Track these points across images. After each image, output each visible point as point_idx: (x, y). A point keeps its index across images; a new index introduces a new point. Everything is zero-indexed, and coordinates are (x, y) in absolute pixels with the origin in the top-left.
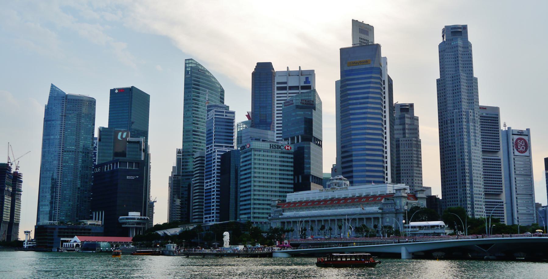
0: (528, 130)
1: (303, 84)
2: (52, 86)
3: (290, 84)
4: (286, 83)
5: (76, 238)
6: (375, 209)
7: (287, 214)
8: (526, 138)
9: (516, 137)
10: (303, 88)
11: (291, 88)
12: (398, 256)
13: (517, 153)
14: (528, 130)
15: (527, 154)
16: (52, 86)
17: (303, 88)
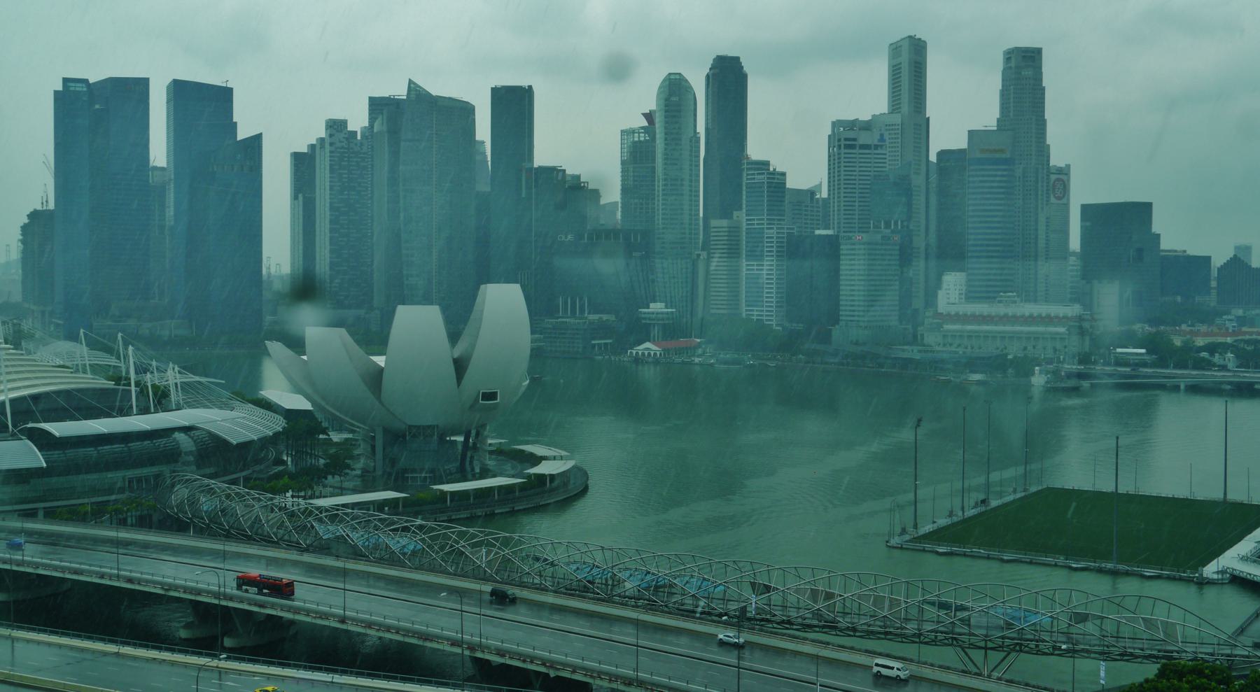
0: (1068, 166)
1: (876, 142)
2: (410, 82)
3: (861, 142)
4: (855, 140)
5: (648, 345)
6: (1062, 330)
7: (946, 327)
8: (1064, 177)
9: (1053, 177)
10: (876, 147)
11: (863, 147)
12: (1176, 388)
13: (1053, 200)
14: (1068, 166)
15: (1064, 201)
16: (410, 82)
17: (876, 147)
